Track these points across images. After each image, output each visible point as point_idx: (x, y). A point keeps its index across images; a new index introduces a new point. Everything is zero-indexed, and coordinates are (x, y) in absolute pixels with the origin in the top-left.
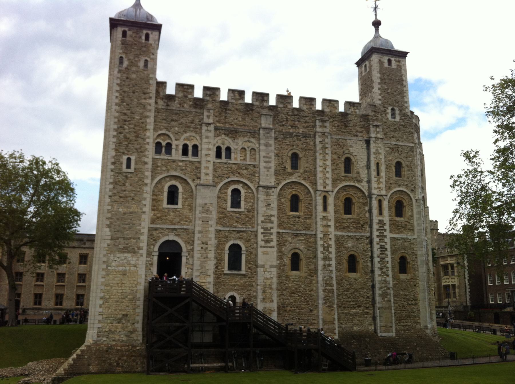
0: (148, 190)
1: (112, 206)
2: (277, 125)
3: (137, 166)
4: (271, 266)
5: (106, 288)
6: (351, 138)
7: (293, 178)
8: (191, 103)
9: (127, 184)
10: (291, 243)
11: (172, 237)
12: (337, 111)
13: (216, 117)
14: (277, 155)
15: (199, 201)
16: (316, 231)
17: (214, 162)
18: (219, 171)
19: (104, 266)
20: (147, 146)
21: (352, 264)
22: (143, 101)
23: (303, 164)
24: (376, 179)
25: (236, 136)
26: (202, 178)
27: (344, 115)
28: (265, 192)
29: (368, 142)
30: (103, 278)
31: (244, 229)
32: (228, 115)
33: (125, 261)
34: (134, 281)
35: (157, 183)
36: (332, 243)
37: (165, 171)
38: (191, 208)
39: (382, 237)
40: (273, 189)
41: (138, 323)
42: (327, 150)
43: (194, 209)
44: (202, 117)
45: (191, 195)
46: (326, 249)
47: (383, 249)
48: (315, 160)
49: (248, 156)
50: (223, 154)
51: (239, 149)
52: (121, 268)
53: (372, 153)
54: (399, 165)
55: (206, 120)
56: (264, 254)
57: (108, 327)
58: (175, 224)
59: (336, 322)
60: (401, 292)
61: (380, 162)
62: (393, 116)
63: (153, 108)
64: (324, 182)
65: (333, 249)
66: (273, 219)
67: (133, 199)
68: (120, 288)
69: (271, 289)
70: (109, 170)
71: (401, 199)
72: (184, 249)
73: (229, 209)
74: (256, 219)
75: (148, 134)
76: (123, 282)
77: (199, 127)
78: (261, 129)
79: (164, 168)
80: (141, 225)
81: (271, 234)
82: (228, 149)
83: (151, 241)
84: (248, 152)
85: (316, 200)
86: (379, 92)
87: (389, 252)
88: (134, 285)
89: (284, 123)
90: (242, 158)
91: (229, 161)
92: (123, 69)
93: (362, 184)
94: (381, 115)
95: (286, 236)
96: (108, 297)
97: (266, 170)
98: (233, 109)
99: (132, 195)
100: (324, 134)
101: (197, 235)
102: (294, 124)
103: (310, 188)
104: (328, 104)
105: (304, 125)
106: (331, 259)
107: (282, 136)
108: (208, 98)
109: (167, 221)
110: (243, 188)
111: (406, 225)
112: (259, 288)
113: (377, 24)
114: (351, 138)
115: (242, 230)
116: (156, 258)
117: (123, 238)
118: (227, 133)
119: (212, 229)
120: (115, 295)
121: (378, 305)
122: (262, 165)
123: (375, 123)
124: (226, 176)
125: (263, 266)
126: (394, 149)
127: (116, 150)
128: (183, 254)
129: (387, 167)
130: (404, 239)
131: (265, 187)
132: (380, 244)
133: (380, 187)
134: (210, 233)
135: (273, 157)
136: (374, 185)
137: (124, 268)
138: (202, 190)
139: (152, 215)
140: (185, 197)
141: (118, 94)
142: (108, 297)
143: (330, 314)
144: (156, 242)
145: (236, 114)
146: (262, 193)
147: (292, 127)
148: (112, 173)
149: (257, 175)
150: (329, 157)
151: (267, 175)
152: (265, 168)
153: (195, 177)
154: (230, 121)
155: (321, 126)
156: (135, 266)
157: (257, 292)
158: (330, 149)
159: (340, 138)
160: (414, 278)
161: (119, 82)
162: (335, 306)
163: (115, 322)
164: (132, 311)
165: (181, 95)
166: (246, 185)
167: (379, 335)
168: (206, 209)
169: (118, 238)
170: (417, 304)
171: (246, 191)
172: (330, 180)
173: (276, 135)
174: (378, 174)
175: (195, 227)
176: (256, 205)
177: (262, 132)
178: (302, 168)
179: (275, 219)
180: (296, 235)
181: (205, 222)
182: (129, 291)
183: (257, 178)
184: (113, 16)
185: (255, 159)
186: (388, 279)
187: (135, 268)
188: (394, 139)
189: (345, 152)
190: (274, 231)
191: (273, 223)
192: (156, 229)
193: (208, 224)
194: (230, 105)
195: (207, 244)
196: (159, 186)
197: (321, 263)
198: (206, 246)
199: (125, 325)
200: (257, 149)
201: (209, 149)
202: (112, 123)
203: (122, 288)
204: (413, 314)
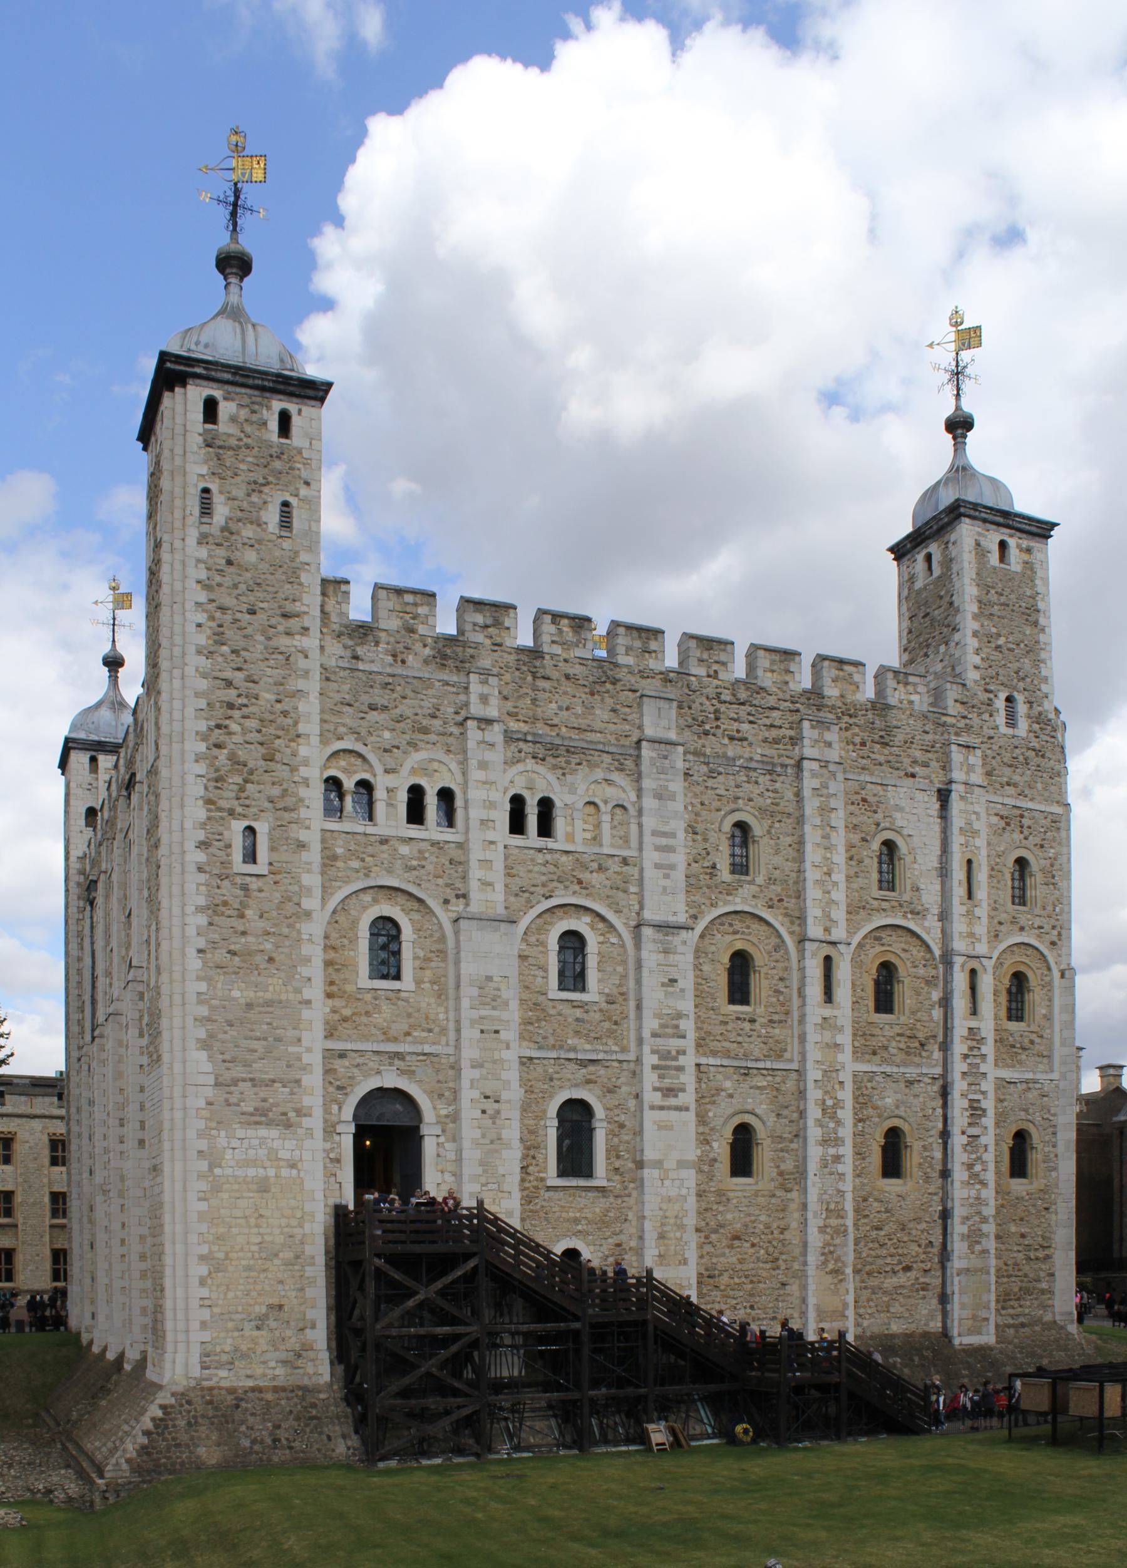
2: (687, 733)
7: (738, 900)
11: (390, 1080)
13: (506, 698)
15: (469, 968)
17: (505, 847)
18: (521, 874)
23: (766, 855)
25: (568, 762)
26: (472, 895)
27: (880, 706)
28: (661, 942)
32: (541, 695)
34: (293, 1209)
37: (358, 871)
38: (445, 990)
40: (683, 934)
42: (833, 815)
43: (451, 992)
44: (463, 697)
45: (439, 952)
48: (800, 844)
49: (606, 827)
50: (532, 821)
51: (580, 805)
52: (252, 1172)
55: (476, 709)
57: (229, 1341)
58: (395, 1040)
68: (256, 1230)
73: (554, 993)
76: (262, 1211)
77: (456, 730)
78: (644, 744)
82: (546, 806)
83: (331, 1089)
84: (606, 818)
88: (294, 1222)
89: (707, 727)
90: (588, 835)
91: (549, 843)
94: (979, 715)
97: (660, 873)
98: (555, 675)
100: (825, 764)
101: (468, 1074)
102: (738, 731)
105: (767, 734)
107: (704, 769)
109: (374, 1031)
110: (592, 928)
115: (594, 1057)
120: (242, 1250)
122: (650, 857)
123: (964, 739)
124: (540, 890)
131: (658, 926)
135: (681, 835)
137: (261, 1171)
139: (328, 1010)
140: (421, 954)
142: (221, 1255)
144: (346, 1094)
145: (566, 693)
147: (732, 738)
151: (665, 888)
152: (657, 866)
153: (449, 893)
156: (293, 1166)
158: (841, 813)
159: (868, 779)
163: (247, 1326)
164: (294, 1294)
166: (603, 919)
171: (601, 939)
173: (687, 765)
175: (458, 1047)
177: (647, 751)
178: (763, 871)
181: (488, 1032)
182: (280, 1239)
185: (626, 839)
187: (294, 1172)
192: (342, 1055)
193: (501, 1042)
196: (341, 918)
199: (277, 1333)
200: (632, 811)
201: (492, 805)
202: (190, 711)
203: (262, 1231)
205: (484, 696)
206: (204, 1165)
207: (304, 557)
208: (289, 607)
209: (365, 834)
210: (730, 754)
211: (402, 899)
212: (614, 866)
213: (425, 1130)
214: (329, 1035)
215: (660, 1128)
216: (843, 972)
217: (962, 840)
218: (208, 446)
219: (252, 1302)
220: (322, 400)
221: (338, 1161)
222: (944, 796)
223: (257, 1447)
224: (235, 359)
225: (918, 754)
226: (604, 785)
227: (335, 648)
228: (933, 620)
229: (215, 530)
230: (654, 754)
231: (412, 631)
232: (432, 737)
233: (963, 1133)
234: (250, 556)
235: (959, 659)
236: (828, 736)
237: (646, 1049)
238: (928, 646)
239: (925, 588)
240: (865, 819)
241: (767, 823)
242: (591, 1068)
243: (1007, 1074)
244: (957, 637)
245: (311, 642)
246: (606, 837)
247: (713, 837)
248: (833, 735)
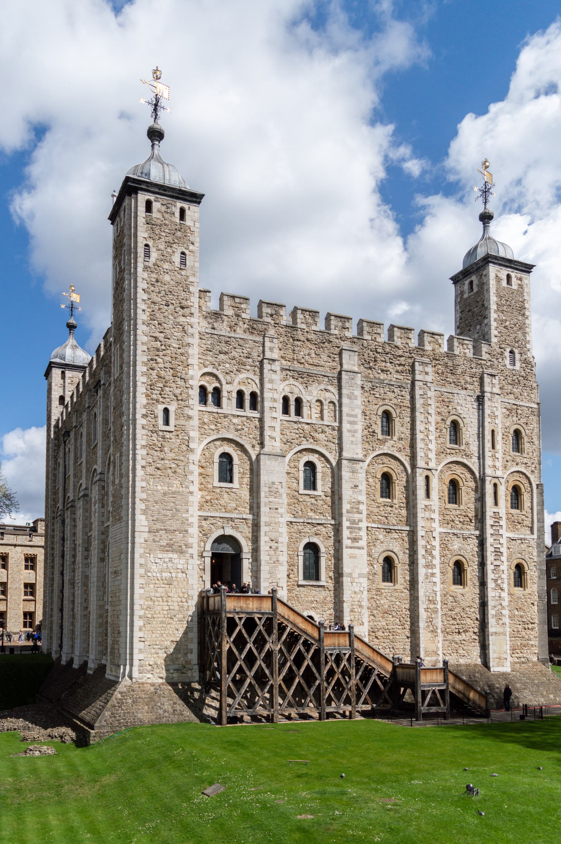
0: (196, 457)
2: (362, 367)
5: (146, 603)
6: (459, 392)
7: (385, 448)
8: (246, 326)
9: (166, 449)
10: (382, 543)
30: (140, 588)
31: (323, 522)
32: (296, 349)
33: (170, 565)
35: (203, 450)
36: (436, 543)
37: (213, 430)
39: (497, 535)
41: (191, 653)
46: (429, 552)
47: (498, 553)
49: (325, 412)
52: (164, 575)
54: (517, 434)
57: (152, 659)
58: (230, 512)
61: (495, 430)
65: (436, 553)
66: (363, 507)
67: (175, 472)
68: (166, 603)
71: (518, 483)
76: (169, 594)
79: (213, 427)
80: (187, 511)
81: (360, 529)
82: (298, 401)
84: (325, 407)
88: (184, 600)
93: (472, 461)
95: (377, 533)
98: (302, 338)
105: (398, 368)
107: (370, 385)
109: (220, 507)
114: (459, 392)
117: (165, 530)
118: (296, 375)
124: (296, 441)
131: (350, 460)
132: (495, 546)
134: (281, 526)
135: (360, 416)
136: (489, 462)
137: (169, 574)
138: (268, 462)
139: (199, 497)
142: (149, 616)
144: (207, 538)
146: (347, 469)
147: (382, 371)
150: (433, 419)
151: (352, 442)
152: (349, 431)
154: (300, 357)
158: (433, 407)
169: (158, 531)
172: (434, 452)
174: (493, 447)
177: (344, 376)
178: (397, 434)
179: (363, 507)
187: (184, 575)
189: (451, 413)
190: (364, 525)
191: (361, 513)
193: (279, 513)
194: (299, 332)
195: (277, 543)
198: (276, 545)
201: (275, 400)
203: (169, 604)
204: (531, 643)
206: (142, 571)
207: (191, 279)
208: (184, 303)
209: (217, 413)
210: (382, 378)
213: (244, 556)
215: (350, 557)
216: (434, 483)
217: (489, 420)
218: (148, 224)
219: (163, 639)
220: (199, 203)
222: (480, 400)
223: (166, 714)
224: (161, 182)
225: (468, 379)
226: (325, 392)
227: (204, 323)
228: (473, 313)
229: (151, 265)
230: (347, 377)
231: (238, 316)
233: (492, 564)
234: (167, 278)
235: (487, 332)
237: (344, 519)
238: (470, 326)
239: (469, 297)
240: (444, 410)
241: (398, 411)
242: (319, 527)
243: (511, 535)
244: (486, 321)
245: (193, 320)
248: (429, 369)
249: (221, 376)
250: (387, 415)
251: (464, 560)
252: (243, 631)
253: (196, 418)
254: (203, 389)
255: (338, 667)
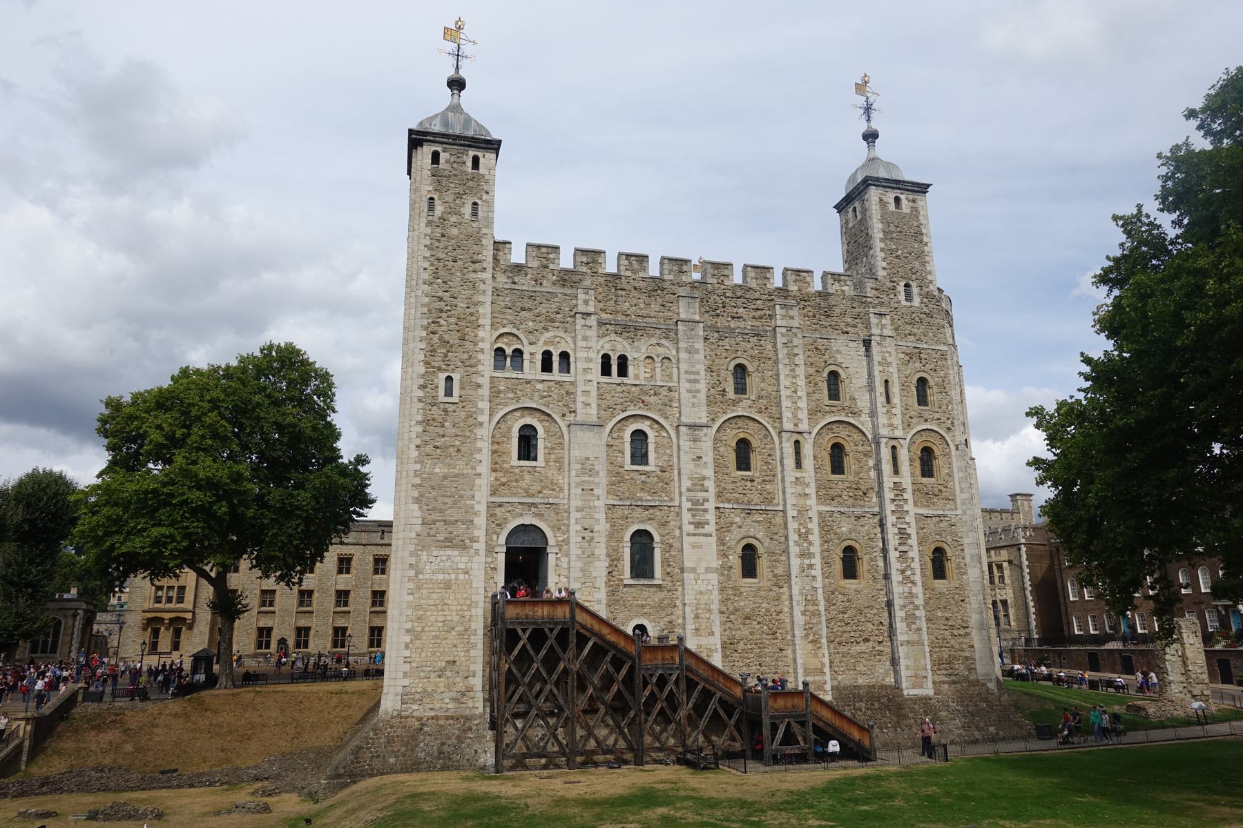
0: (485, 432)
1: (421, 463)
2: (707, 315)
3: (463, 392)
4: (708, 570)
9: (447, 424)
10: (740, 527)
11: (528, 520)
12: (810, 289)
14: (710, 369)
15: (576, 453)
16: (785, 505)
19: (412, 573)
20: (480, 356)
21: (850, 563)
22: (472, 275)
23: (754, 383)
24: (884, 410)
27: (824, 295)
29: (867, 344)
33: (447, 564)
36: (814, 526)
39: (900, 513)
43: (566, 467)
46: (804, 537)
47: (903, 535)
48: (777, 376)
49: (658, 370)
52: (441, 577)
53: (876, 363)
55: (581, 308)
56: (693, 547)
59: (827, 670)
60: (940, 614)
62: (909, 297)
63: (488, 287)
64: (795, 416)
65: (815, 538)
66: (706, 483)
69: (710, 611)
70: (415, 400)
71: (929, 444)
72: (551, 541)
73: (628, 466)
74: (677, 485)
75: (481, 334)
77: (570, 320)
79: (511, 395)
81: (706, 511)
82: (623, 360)
85: (781, 449)
86: (883, 255)
87: (913, 541)
88: (465, 608)
91: (625, 380)
92: (435, 219)
96: (419, 629)
97: (690, 395)
98: (628, 287)
99: (457, 443)
100: (790, 329)
101: (574, 515)
103: (768, 426)
104: (794, 277)
106: (813, 554)
107: (716, 335)
108: (584, 269)
111: (940, 491)
112: (687, 609)
113: (871, 137)
116: (501, 558)
118: (619, 330)
119: (600, 504)
121: (901, 637)
122: (685, 386)
125: (693, 570)
126: (912, 356)
127: (427, 363)
128: (549, 550)
129: (904, 387)
130: (939, 516)
133: (894, 423)
135: (703, 373)
136: (882, 420)
138: (580, 434)
141: (426, 265)
142: (419, 629)
143: (816, 656)
146: (686, 437)
147: (733, 318)
148: (421, 405)
149: (675, 405)
150: (801, 371)
152: (689, 391)
155: (783, 317)
156: (467, 573)
157: (684, 618)
158: (801, 356)
160: (961, 588)
161: (428, 242)
162: (824, 641)
163: (433, 675)
165: (535, 264)
166: (657, 422)
167: (905, 693)
168: (587, 468)
170: (967, 634)
174: (888, 401)
176: (675, 460)
177: (681, 327)
179: (710, 484)
180: (749, 513)
182: (456, 619)
183: (676, 411)
184: (414, 126)
185: (670, 377)
186: (915, 590)
188: (912, 338)
192: (500, 505)
197: (795, 562)
201: (589, 360)
205: (585, 301)
211: (538, 415)
212: (664, 392)
214: (493, 494)
221: (495, 569)
232: (557, 324)
236: (791, 313)
246: (658, 377)
247: (723, 373)
249: (521, 336)
250: (741, 370)
251: (857, 546)
252: (528, 647)
253: (487, 386)
254: (500, 352)
255: (661, 690)
